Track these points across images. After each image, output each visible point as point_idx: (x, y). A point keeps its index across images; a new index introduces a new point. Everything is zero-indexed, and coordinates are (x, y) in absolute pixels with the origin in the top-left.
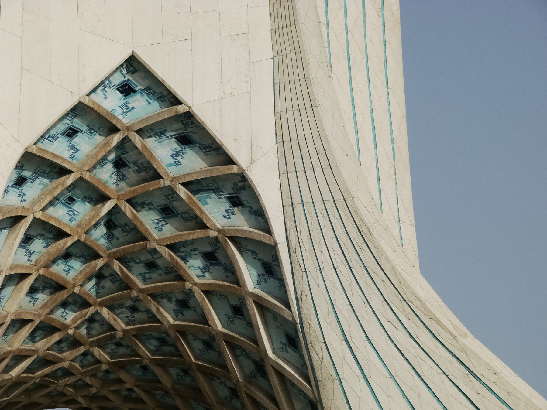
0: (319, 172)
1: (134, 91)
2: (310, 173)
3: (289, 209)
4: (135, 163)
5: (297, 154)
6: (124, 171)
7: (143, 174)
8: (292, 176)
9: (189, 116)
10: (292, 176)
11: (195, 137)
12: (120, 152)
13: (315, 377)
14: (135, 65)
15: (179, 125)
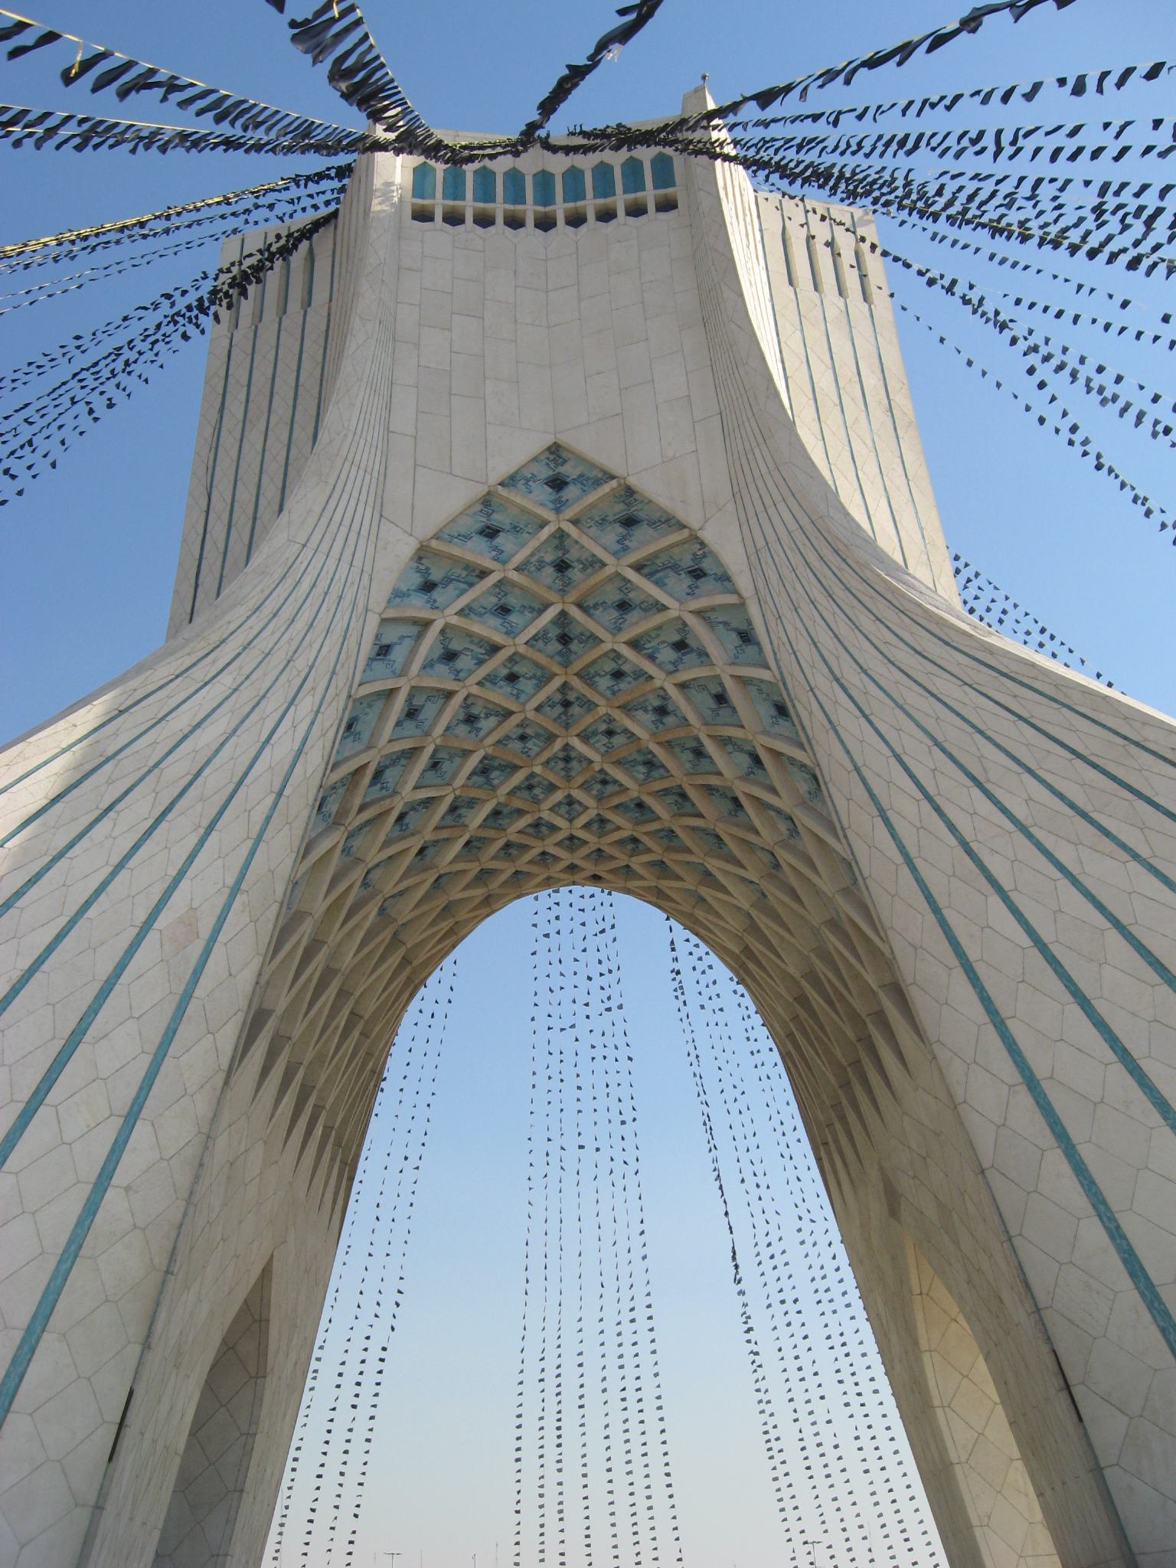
0: (781, 506)
1: (566, 484)
2: (772, 510)
3: (753, 558)
4: (579, 561)
5: (755, 495)
6: (570, 573)
7: (589, 571)
8: (753, 521)
9: (629, 493)
10: (753, 521)
11: (642, 515)
12: (560, 554)
13: (807, 737)
14: (564, 455)
15: (622, 506)
